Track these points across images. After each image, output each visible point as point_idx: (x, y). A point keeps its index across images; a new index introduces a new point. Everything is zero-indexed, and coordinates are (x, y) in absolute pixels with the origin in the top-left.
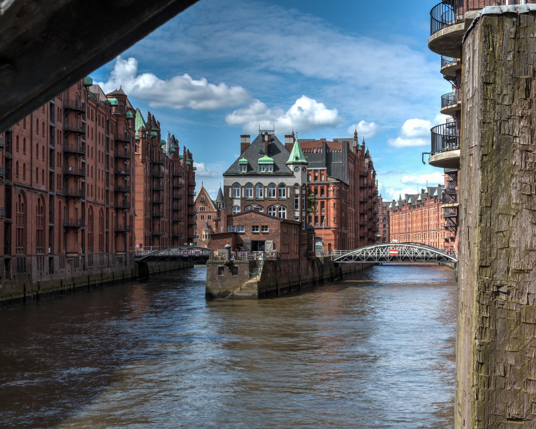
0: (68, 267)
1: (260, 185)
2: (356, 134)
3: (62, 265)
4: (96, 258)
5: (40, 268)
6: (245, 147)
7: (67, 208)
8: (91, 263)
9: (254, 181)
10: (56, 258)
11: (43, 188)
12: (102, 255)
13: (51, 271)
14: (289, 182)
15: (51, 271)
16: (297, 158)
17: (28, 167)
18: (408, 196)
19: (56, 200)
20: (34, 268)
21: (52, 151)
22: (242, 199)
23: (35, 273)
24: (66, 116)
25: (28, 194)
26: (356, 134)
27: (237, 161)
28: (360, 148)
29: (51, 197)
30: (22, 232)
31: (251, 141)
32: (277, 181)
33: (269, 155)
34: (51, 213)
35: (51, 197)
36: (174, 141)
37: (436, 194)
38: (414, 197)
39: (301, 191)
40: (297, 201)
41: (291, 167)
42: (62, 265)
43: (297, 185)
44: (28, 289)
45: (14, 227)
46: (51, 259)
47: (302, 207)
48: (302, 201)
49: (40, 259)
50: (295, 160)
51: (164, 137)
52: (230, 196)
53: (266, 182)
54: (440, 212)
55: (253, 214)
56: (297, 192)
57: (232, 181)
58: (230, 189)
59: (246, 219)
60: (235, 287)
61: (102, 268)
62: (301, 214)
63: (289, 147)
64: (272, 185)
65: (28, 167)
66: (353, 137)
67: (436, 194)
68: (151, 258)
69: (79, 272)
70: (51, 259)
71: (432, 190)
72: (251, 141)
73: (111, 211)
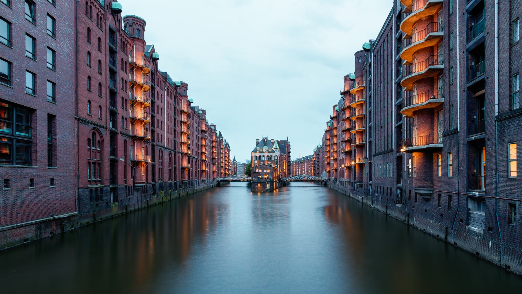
0: (202, 184)
1: (264, 156)
2: (288, 138)
3: (201, 184)
4: (209, 181)
5: (196, 184)
6: (258, 143)
7: (202, 164)
8: (207, 182)
9: (262, 154)
10: (200, 181)
11: (197, 157)
12: (210, 180)
13: (199, 186)
14: (274, 155)
15: (199, 186)
16: (276, 147)
17: (193, 150)
18: (298, 159)
19: (200, 161)
20: (195, 185)
21: (198, 145)
23: (195, 186)
24: (202, 133)
25: (193, 159)
26: (288, 138)
27: (256, 148)
28: (289, 143)
29: (199, 160)
30: (192, 172)
31: (260, 141)
32: (270, 154)
34: (199, 166)
35: (199, 160)
36: (225, 141)
37: (309, 158)
38: (300, 159)
40: (276, 161)
42: (201, 184)
43: (276, 156)
44: (194, 192)
45: (190, 170)
46: (199, 181)
49: (196, 181)
51: (224, 140)
55: (264, 166)
56: (276, 158)
57: (254, 154)
59: (262, 167)
61: (210, 184)
63: (273, 143)
65: (193, 150)
66: (287, 139)
67: (309, 158)
68: (222, 181)
69: (205, 186)
70: (199, 181)
71: (307, 157)
72: (260, 141)
73: (212, 165)
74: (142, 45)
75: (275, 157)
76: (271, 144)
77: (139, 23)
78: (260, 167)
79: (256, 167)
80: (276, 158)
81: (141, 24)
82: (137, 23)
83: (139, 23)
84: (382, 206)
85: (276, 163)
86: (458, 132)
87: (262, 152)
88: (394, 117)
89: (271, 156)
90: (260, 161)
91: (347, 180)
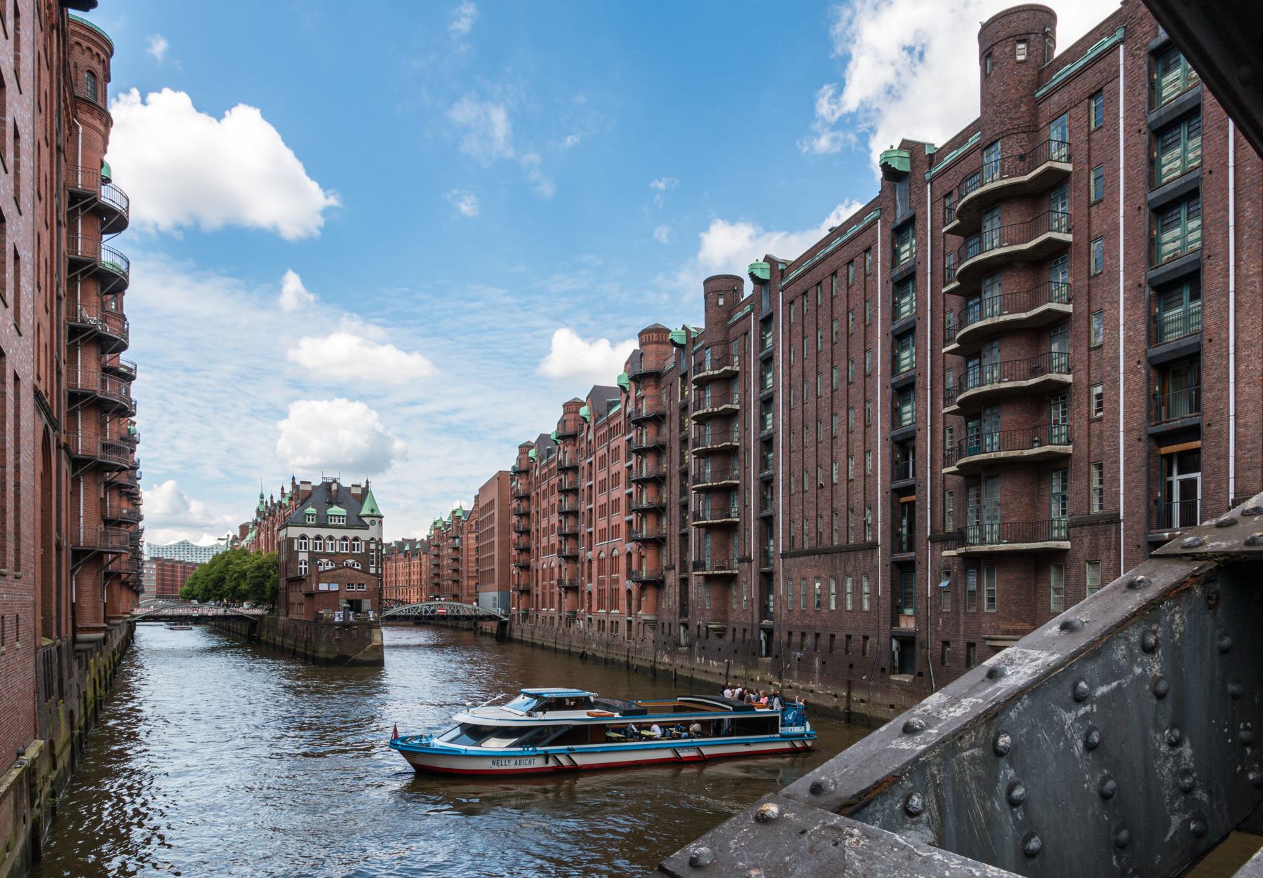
1: (331, 538)
9: (324, 533)
22: (309, 552)
32: (351, 534)
33: (338, 504)
39: (377, 546)
41: (367, 520)
43: (372, 539)
47: (377, 564)
48: (377, 556)
50: (370, 513)
52: (296, 549)
53: (338, 534)
54: (414, 577)
55: (348, 570)
58: (296, 541)
59: (340, 576)
60: (357, 651)
62: (377, 570)
64: (345, 539)
74: (102, 128)
75: (368, 543)
76: (353, 501)
77: (95, 50)
78: (335, 576)
79: (321, 576)
80: (373, 546)
81: (103, 56)
82: (89, 49)
83: (95, 50)
84: (825, 681)
85: (372, 563)
86: (1120, 521)
87: (326, 526)
88: (882, 466)
89: (356, 539)
90: (318, 553)
91: (648, 618)
